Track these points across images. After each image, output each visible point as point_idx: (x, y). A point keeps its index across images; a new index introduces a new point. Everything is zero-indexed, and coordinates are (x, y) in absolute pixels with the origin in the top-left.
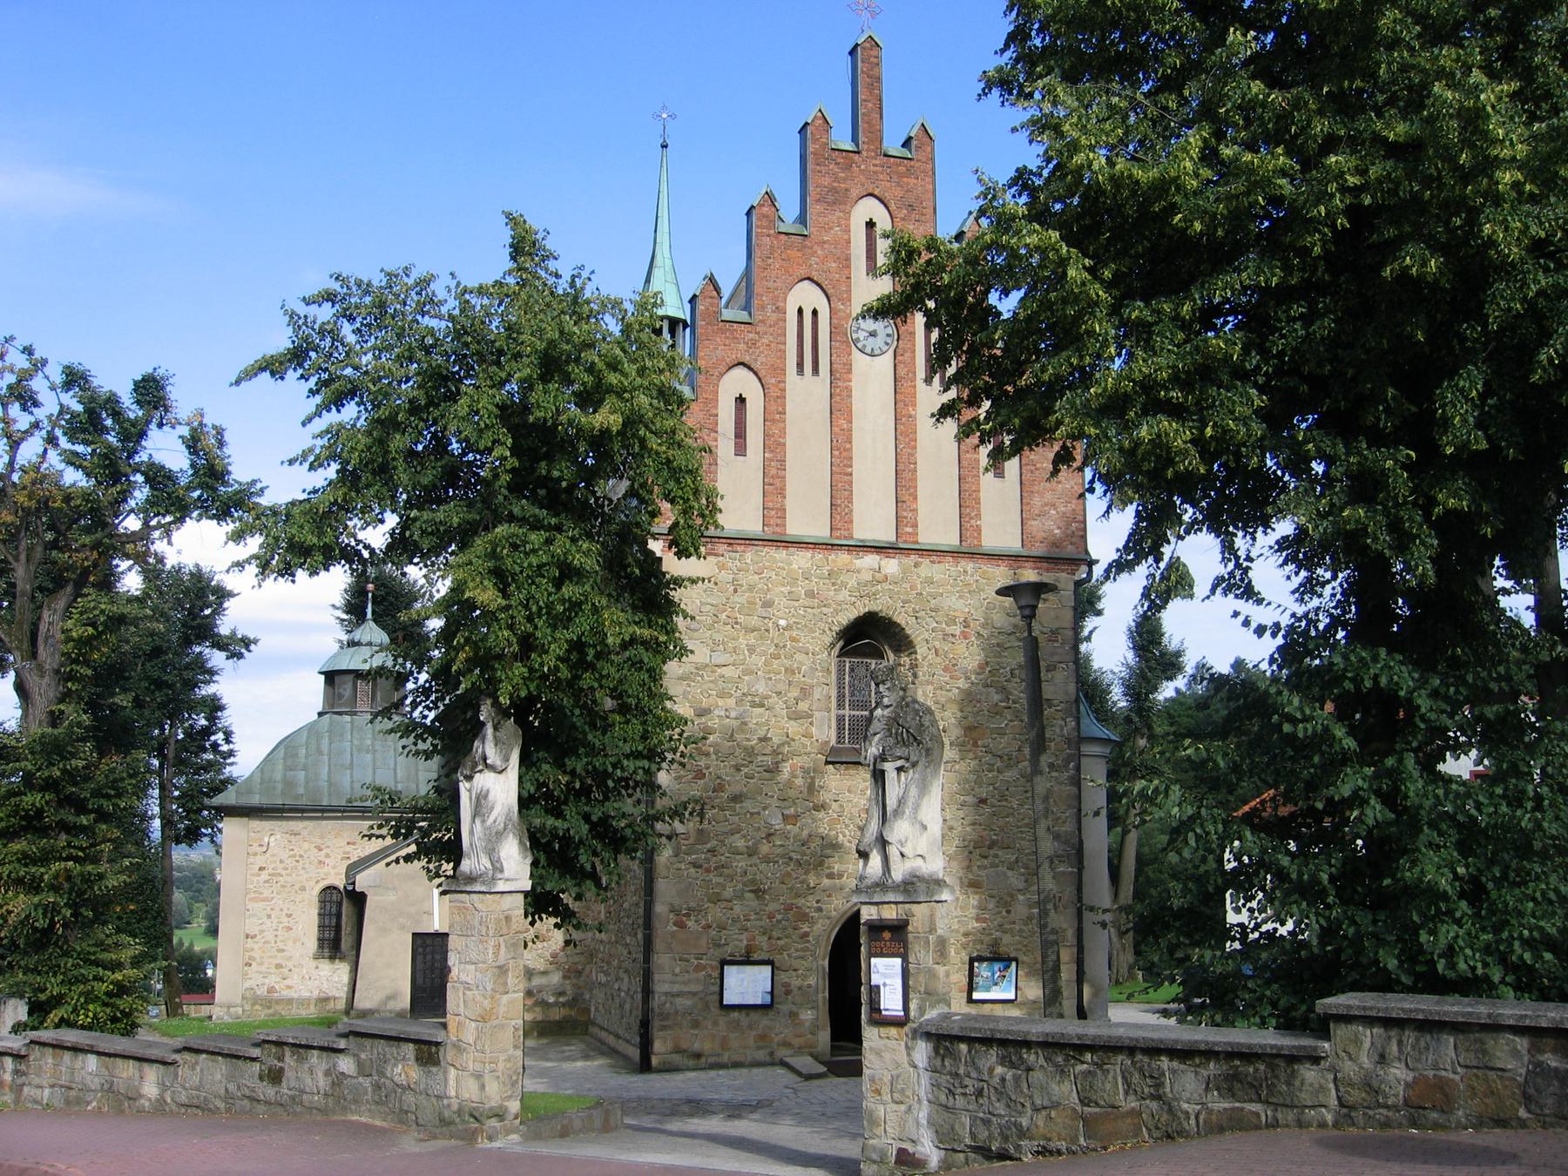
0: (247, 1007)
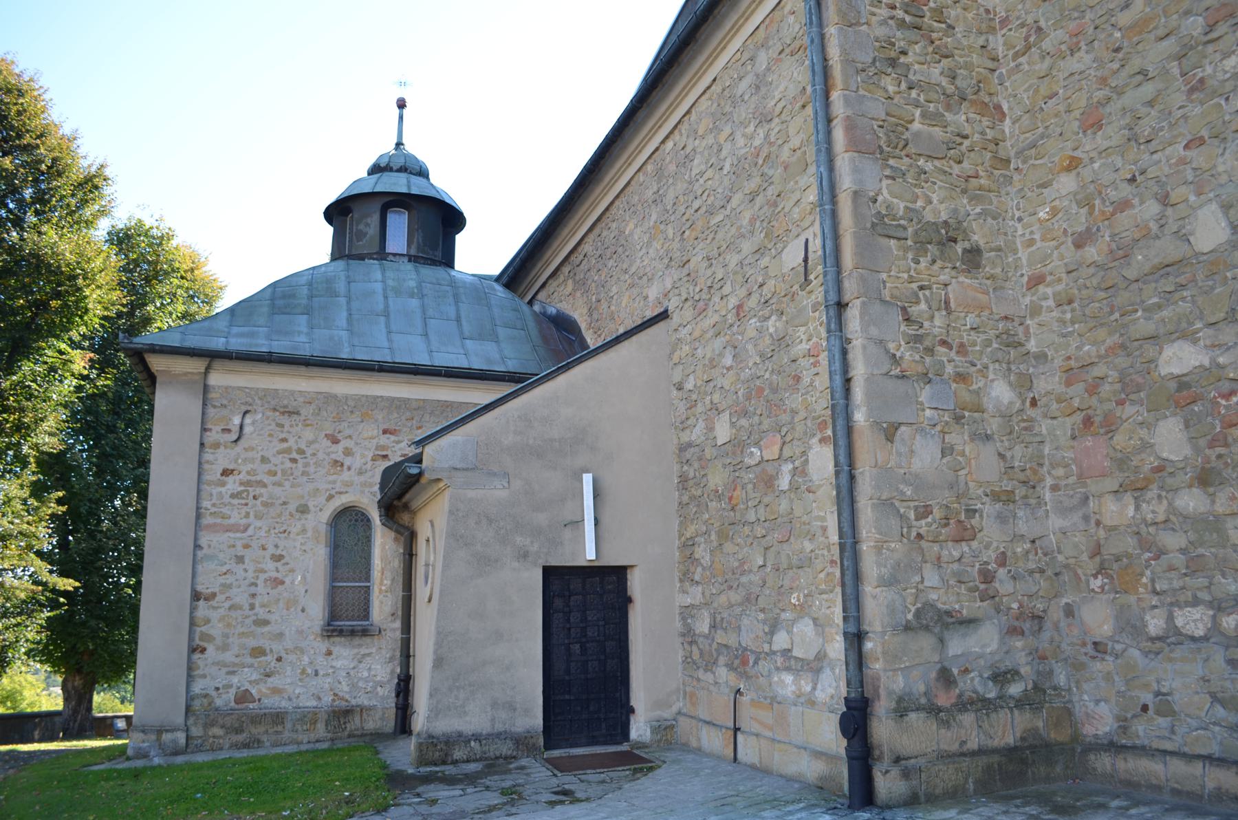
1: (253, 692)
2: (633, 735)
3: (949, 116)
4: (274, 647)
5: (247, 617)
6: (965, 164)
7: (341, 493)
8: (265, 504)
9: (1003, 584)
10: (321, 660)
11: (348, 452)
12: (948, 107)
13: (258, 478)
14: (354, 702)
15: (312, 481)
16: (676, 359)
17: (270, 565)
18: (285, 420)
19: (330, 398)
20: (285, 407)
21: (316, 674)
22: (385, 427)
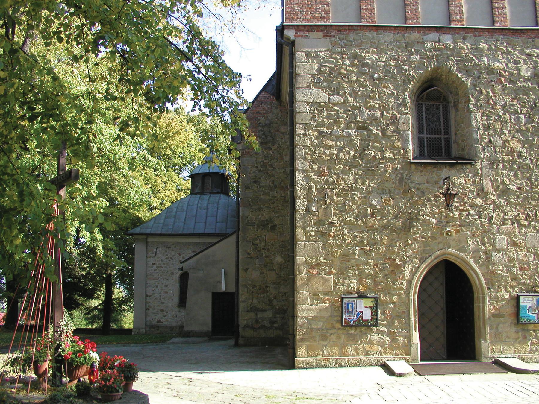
0: (148, 329)
3: (271, 193)
6: (275, 204)
8: (163, 272)
9: (275, 302)
10: (178, 313)
12: (271, 190)
17: (165, 288)
18: (167, 250)
19: (179, 243)
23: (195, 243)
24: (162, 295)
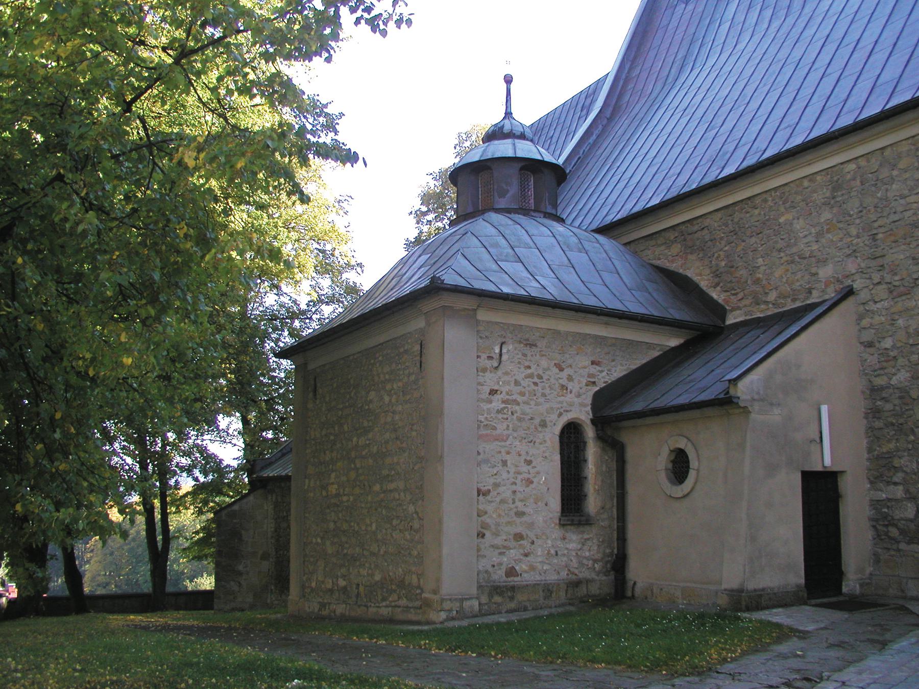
0: (484, 599)
1: (517, 568)
2: (845, 589)
4: (529, 533)
5: (511, 509)
7: (567, 411)
8: (519, 419)
10: (559, 543)
11: (570, 378)
13: (514, 397)
14: (581, 576)
15: (547, 401)
16: (865, 323)
17: (525, 468)
18: (528, 351)
19: (557, 333)
20: (528, 340)
21: (557, 554)
22: (592, 359)
23: (596, 337)
24: (519, 488)
